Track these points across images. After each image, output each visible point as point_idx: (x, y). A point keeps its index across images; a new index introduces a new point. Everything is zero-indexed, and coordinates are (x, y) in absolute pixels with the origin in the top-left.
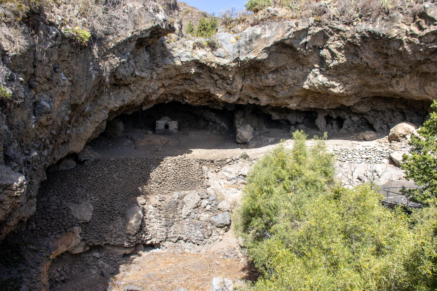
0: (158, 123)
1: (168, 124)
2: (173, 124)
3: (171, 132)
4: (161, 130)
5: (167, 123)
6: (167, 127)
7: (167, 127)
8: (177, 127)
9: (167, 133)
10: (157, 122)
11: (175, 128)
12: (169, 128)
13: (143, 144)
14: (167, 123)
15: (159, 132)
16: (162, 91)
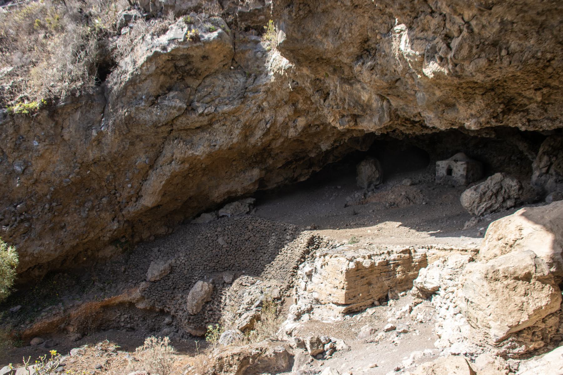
0: (439, 166)
1: (452, 167)
2: (459, 168)
3: (455, 181)
4: (441, 178)
5: (449, 166)
6: (450, 171)
7: (450, 171)
8: (464, 173)
9: (449, 183)
10: (439, 163)
11: (461, 175)
12: (453, 175)
13: (374, 201)
14: (449, 166)
15: (439, 182)
16: (301, 122)
